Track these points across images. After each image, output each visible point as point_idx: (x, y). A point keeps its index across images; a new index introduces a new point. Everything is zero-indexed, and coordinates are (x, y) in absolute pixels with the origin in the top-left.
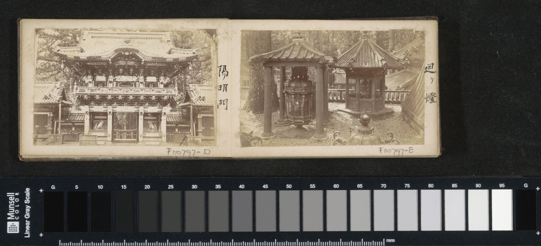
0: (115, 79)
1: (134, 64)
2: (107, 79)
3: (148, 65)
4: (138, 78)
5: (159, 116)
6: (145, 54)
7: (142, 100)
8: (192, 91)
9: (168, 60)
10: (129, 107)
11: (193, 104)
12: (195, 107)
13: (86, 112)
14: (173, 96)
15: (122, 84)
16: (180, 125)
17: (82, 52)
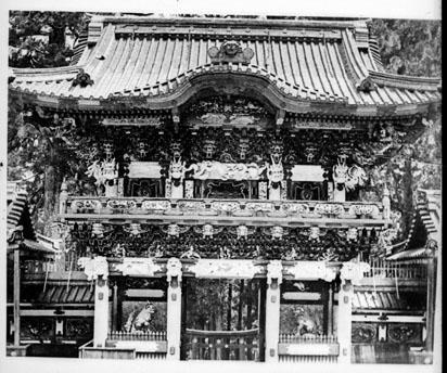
5: (331, 291)
9: (360, 112)
10: (235, 261)
13: (100, 277)
15: (214, 189)
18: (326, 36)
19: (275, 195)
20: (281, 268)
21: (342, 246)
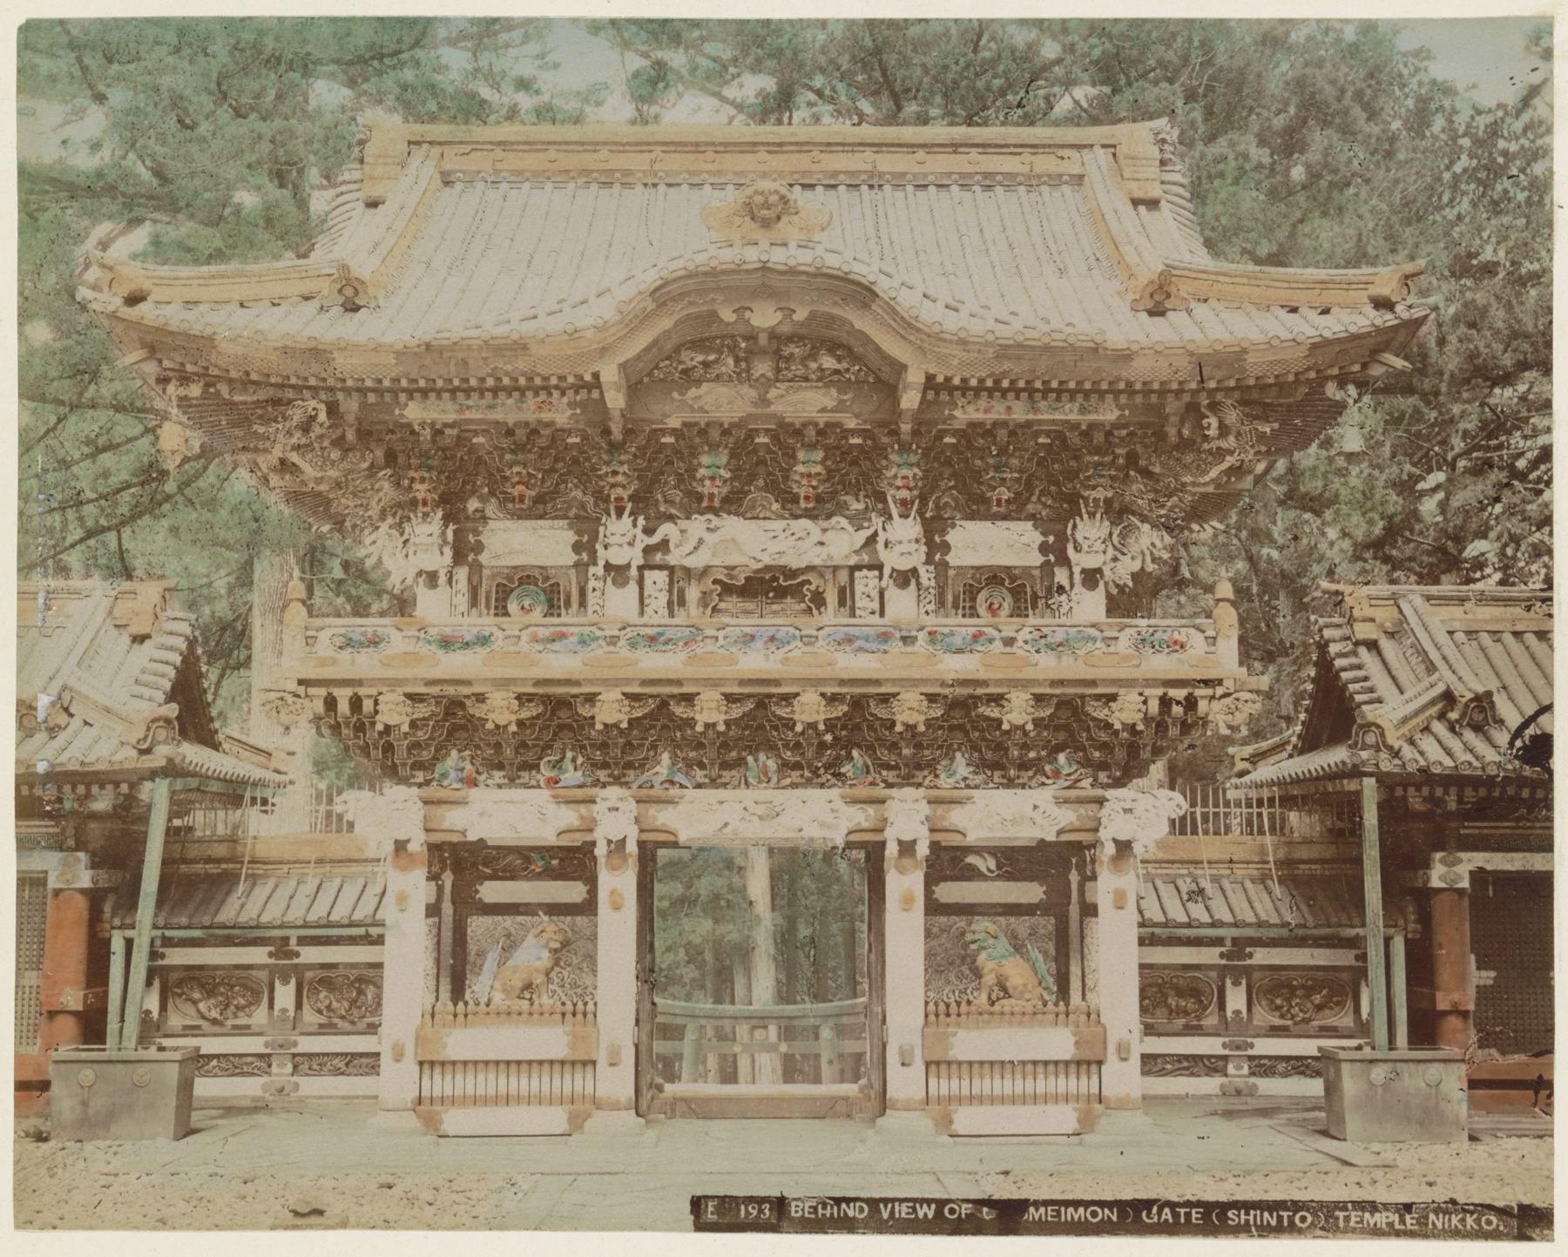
0: (664, 545)
1: (834, 410)
2: (586, 547)
3: (958, 413)
4: (872, 540)
5: (1074, 877)
6: (930, 315)
7: (910, 727)
8: (1373, 645)
9: (1141, 370)
10: (789, 792)
11: (1387, 765)
12: (1399, 792)
13: (400, 846)
14: (1198, 692)
15: (727, 589)
16: (1261, 956)
17: (352, 308)
18: (1038, 169)
19: (903, 605)
20: (925, 809)
21: (1103, 746)
